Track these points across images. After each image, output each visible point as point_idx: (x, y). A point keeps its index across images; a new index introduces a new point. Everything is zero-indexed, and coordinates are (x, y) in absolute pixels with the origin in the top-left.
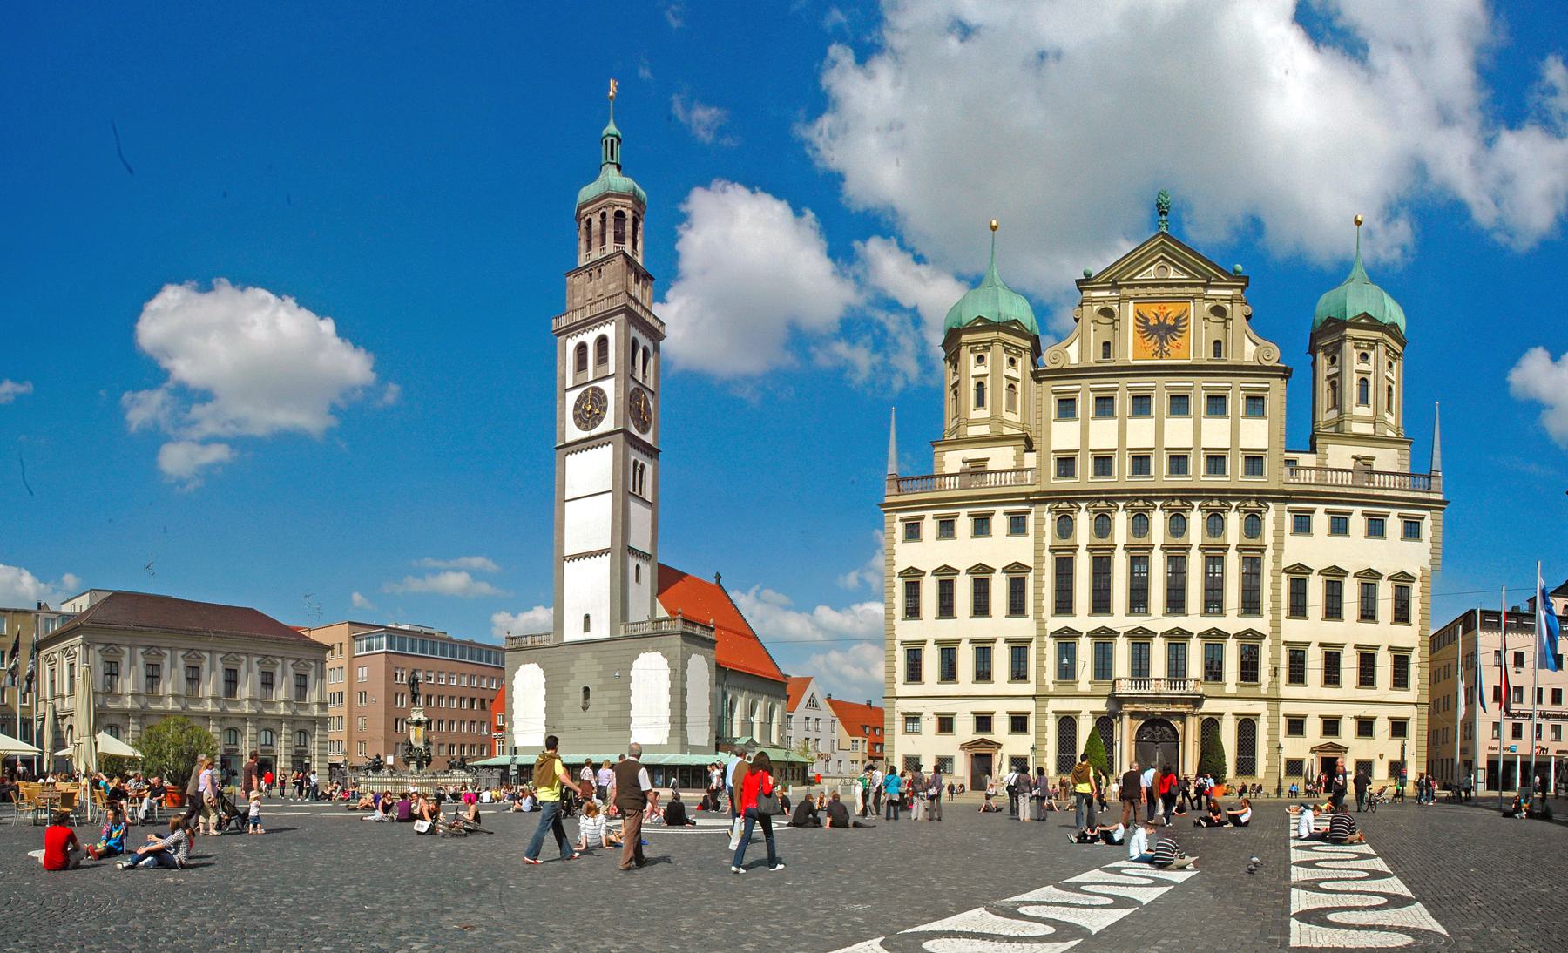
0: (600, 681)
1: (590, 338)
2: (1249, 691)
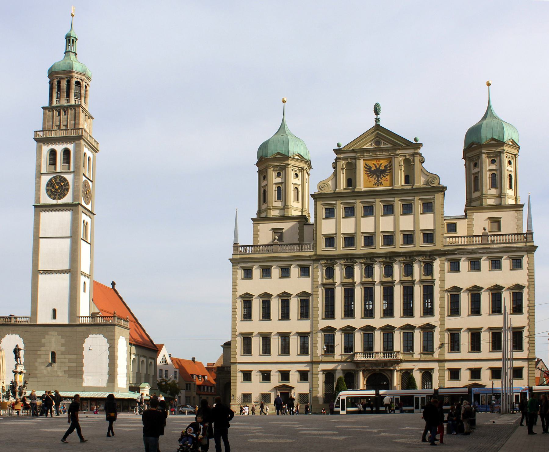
0: (63, 349)
1: (59, 148)
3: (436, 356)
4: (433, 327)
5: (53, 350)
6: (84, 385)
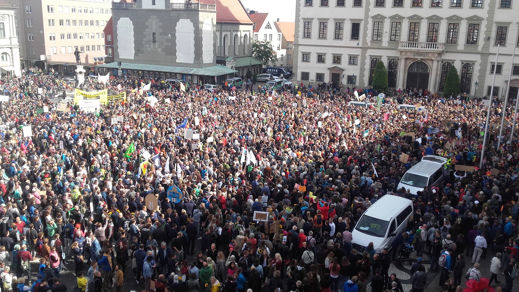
0: (161, 31)
2: (471, 47)
3: (480, 49)
4: (481, 19)
5: (154, 31)
6: (178, 61)
